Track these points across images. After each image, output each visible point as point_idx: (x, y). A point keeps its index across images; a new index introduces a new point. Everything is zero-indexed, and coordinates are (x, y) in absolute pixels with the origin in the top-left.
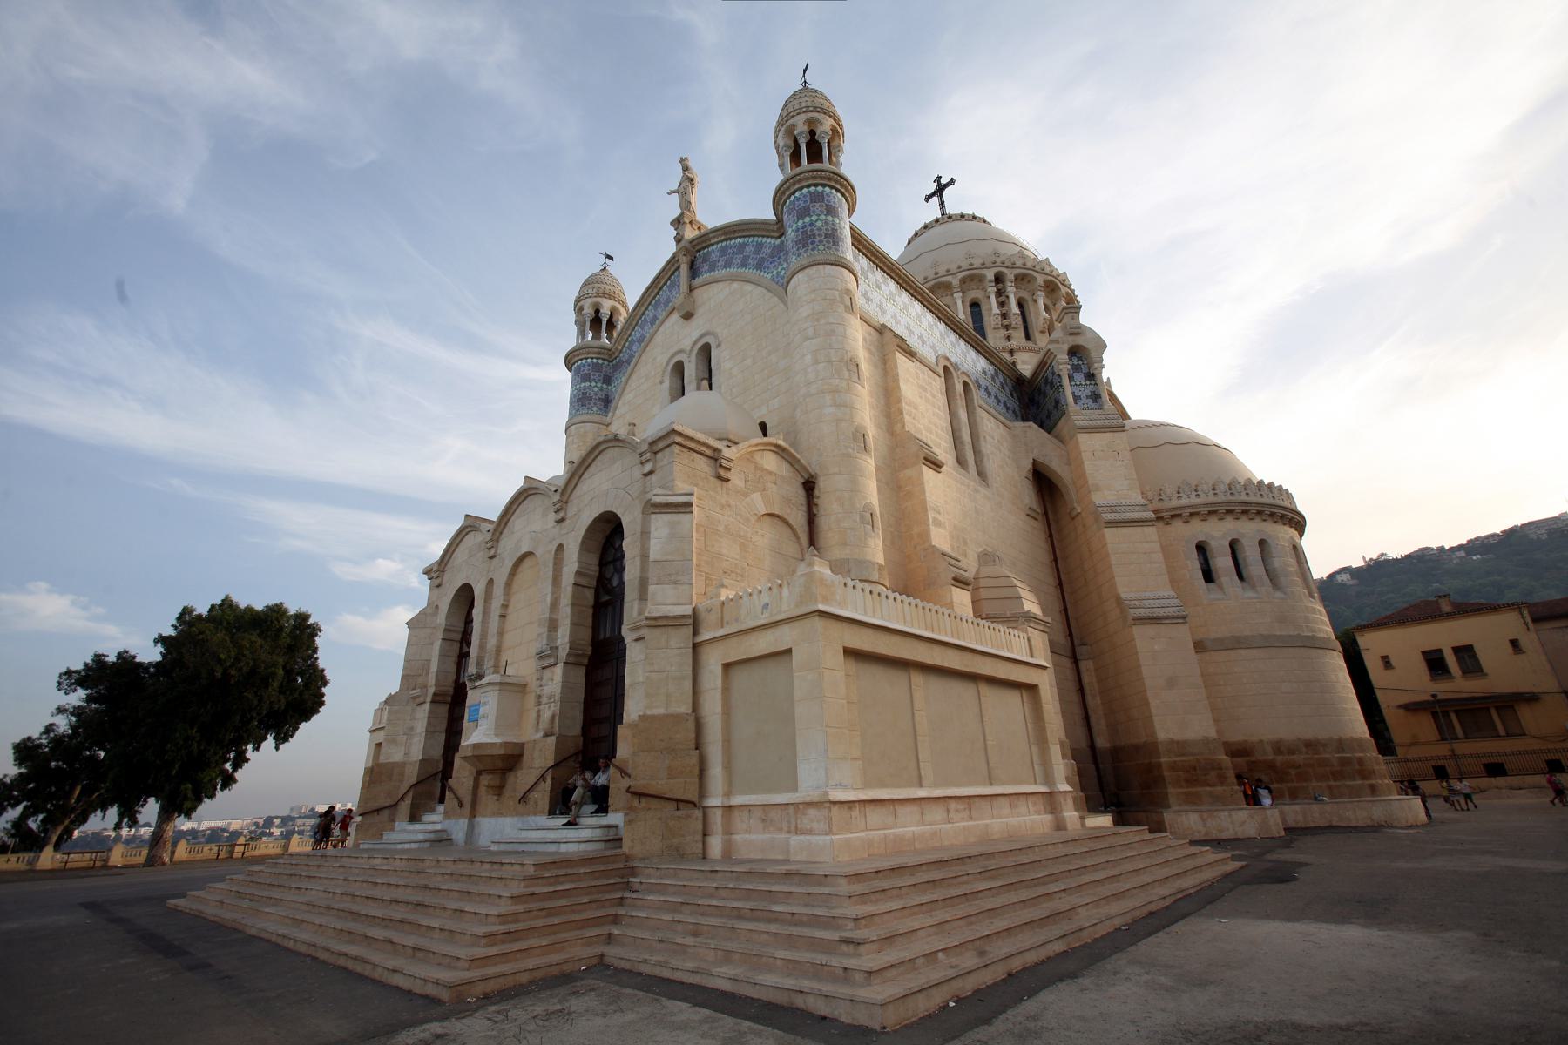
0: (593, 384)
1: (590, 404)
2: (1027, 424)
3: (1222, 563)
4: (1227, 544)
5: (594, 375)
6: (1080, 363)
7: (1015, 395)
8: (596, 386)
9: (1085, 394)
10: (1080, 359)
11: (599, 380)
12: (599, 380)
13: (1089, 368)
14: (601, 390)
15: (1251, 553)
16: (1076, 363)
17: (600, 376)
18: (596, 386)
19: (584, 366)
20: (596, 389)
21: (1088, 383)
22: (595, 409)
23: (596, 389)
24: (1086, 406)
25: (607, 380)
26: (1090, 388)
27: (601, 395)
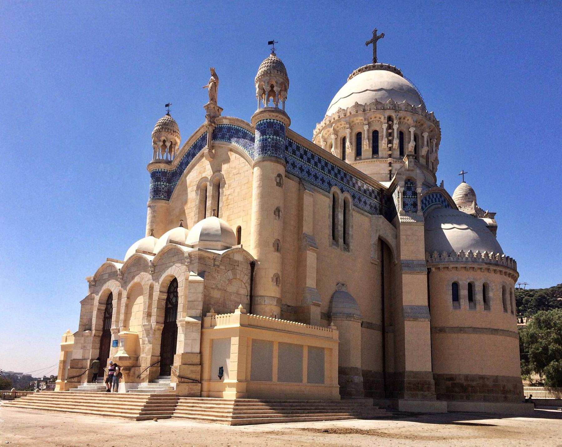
0: (162, 183)
1: (160, 194)
2: (380, 216)
3: (464, 292)
4: (467, 284)
5: (162, 178)
6: (412, 185)
7: (378, 197)
8: (163, 184)
9: (411, 202)
10: (412, 183)
11: (165, 181)
12: (165, 181)
13: (415, 189)
14: (166, 187)
15: (478, 289)
16: (409, 185)
17: (165, 178)
18: (163, 184)
19: (157, 173)
20: (163, 186)
21: (413, 197)
22: (162, 197)
23: (163, 186)
24: (409, 209)
25: (169, 181)
26: (413, 200)
27: (166, 189)
